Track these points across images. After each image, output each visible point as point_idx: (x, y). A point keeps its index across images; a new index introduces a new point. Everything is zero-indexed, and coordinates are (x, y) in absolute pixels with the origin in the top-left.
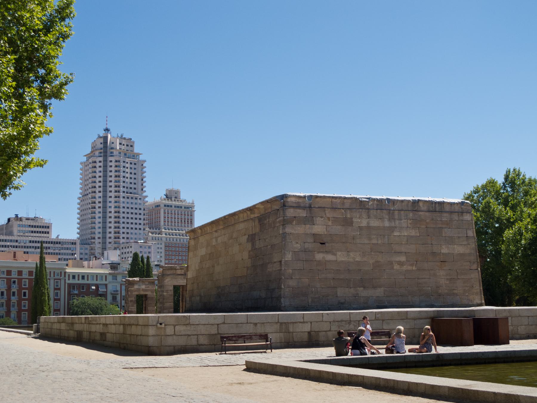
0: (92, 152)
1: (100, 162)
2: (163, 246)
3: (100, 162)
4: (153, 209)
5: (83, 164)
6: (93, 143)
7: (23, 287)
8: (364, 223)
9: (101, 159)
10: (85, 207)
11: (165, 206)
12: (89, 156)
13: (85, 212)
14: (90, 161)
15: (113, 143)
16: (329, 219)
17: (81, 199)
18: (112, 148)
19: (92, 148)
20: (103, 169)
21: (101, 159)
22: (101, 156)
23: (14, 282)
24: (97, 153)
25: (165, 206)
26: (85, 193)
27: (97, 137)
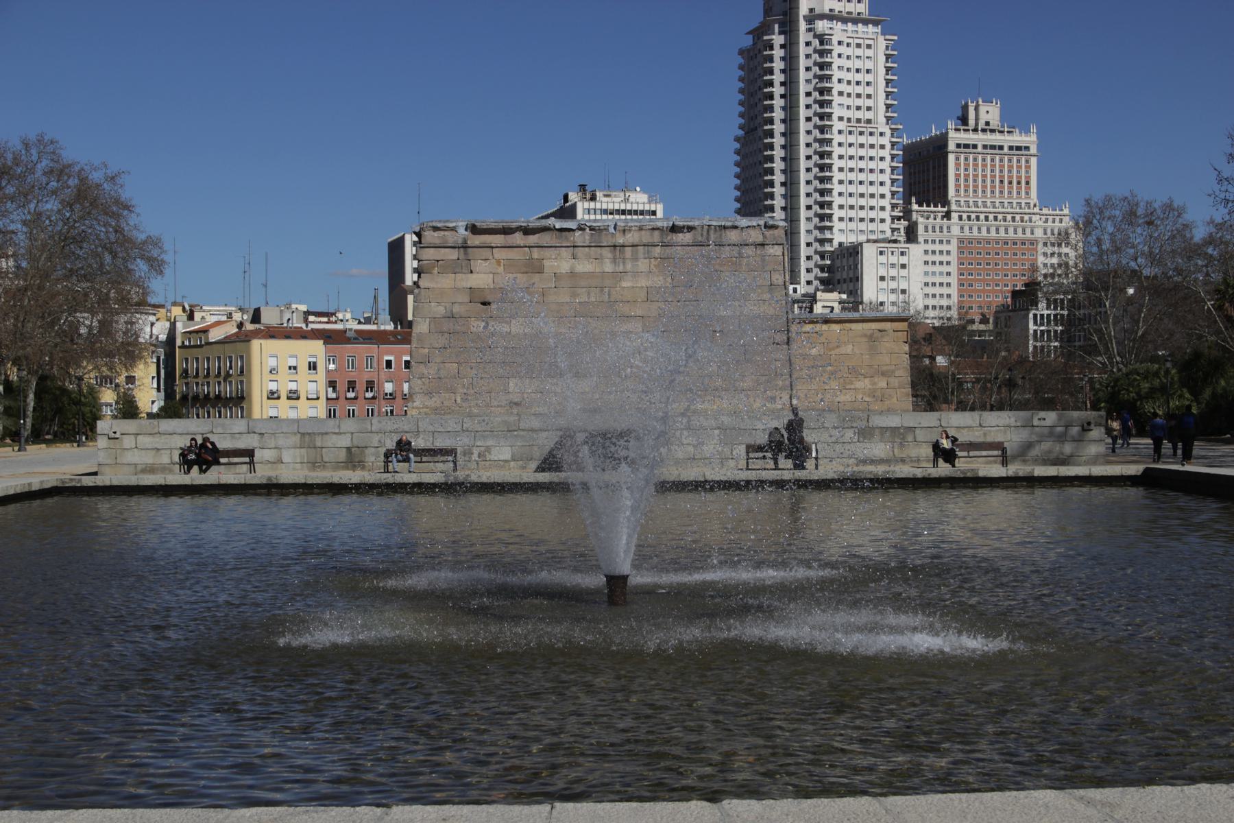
2: (953, 247)
8: (565, 266)
11: (958, 146)
16: (498, 262)
25: (958, 146)
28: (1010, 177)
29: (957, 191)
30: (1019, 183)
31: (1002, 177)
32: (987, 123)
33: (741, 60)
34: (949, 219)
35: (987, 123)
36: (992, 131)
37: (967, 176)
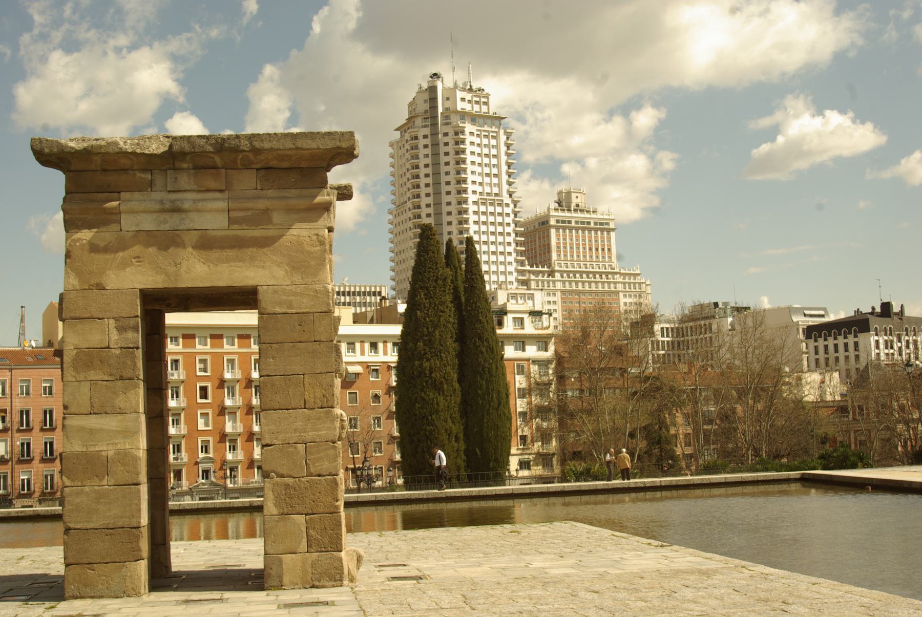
0: (409, 119)
1: (425, 137)
3: (425, 137)
4: (535, 230)
5: (395, 146)
6: (410, 104)
7: (199, 374)
9: (427, 131)
10: (402, 227)
11: (557, 221)
14: (407, 136)
15: (448, 99)
18: (447, 109)
19: (410, 112)
20: (432, 150)
21: (427, 131)
22: (425, 126)
23: (177, 361)
24: (419, 122)
26: (402, 201)
27: (417, 89)
29: (559, 255)
30: (603, 250)
31: (590, 245)
32: (577, 205)
33: (391, 150)
35: (577, 205)
36: (582, 211)
37: (565, 244)
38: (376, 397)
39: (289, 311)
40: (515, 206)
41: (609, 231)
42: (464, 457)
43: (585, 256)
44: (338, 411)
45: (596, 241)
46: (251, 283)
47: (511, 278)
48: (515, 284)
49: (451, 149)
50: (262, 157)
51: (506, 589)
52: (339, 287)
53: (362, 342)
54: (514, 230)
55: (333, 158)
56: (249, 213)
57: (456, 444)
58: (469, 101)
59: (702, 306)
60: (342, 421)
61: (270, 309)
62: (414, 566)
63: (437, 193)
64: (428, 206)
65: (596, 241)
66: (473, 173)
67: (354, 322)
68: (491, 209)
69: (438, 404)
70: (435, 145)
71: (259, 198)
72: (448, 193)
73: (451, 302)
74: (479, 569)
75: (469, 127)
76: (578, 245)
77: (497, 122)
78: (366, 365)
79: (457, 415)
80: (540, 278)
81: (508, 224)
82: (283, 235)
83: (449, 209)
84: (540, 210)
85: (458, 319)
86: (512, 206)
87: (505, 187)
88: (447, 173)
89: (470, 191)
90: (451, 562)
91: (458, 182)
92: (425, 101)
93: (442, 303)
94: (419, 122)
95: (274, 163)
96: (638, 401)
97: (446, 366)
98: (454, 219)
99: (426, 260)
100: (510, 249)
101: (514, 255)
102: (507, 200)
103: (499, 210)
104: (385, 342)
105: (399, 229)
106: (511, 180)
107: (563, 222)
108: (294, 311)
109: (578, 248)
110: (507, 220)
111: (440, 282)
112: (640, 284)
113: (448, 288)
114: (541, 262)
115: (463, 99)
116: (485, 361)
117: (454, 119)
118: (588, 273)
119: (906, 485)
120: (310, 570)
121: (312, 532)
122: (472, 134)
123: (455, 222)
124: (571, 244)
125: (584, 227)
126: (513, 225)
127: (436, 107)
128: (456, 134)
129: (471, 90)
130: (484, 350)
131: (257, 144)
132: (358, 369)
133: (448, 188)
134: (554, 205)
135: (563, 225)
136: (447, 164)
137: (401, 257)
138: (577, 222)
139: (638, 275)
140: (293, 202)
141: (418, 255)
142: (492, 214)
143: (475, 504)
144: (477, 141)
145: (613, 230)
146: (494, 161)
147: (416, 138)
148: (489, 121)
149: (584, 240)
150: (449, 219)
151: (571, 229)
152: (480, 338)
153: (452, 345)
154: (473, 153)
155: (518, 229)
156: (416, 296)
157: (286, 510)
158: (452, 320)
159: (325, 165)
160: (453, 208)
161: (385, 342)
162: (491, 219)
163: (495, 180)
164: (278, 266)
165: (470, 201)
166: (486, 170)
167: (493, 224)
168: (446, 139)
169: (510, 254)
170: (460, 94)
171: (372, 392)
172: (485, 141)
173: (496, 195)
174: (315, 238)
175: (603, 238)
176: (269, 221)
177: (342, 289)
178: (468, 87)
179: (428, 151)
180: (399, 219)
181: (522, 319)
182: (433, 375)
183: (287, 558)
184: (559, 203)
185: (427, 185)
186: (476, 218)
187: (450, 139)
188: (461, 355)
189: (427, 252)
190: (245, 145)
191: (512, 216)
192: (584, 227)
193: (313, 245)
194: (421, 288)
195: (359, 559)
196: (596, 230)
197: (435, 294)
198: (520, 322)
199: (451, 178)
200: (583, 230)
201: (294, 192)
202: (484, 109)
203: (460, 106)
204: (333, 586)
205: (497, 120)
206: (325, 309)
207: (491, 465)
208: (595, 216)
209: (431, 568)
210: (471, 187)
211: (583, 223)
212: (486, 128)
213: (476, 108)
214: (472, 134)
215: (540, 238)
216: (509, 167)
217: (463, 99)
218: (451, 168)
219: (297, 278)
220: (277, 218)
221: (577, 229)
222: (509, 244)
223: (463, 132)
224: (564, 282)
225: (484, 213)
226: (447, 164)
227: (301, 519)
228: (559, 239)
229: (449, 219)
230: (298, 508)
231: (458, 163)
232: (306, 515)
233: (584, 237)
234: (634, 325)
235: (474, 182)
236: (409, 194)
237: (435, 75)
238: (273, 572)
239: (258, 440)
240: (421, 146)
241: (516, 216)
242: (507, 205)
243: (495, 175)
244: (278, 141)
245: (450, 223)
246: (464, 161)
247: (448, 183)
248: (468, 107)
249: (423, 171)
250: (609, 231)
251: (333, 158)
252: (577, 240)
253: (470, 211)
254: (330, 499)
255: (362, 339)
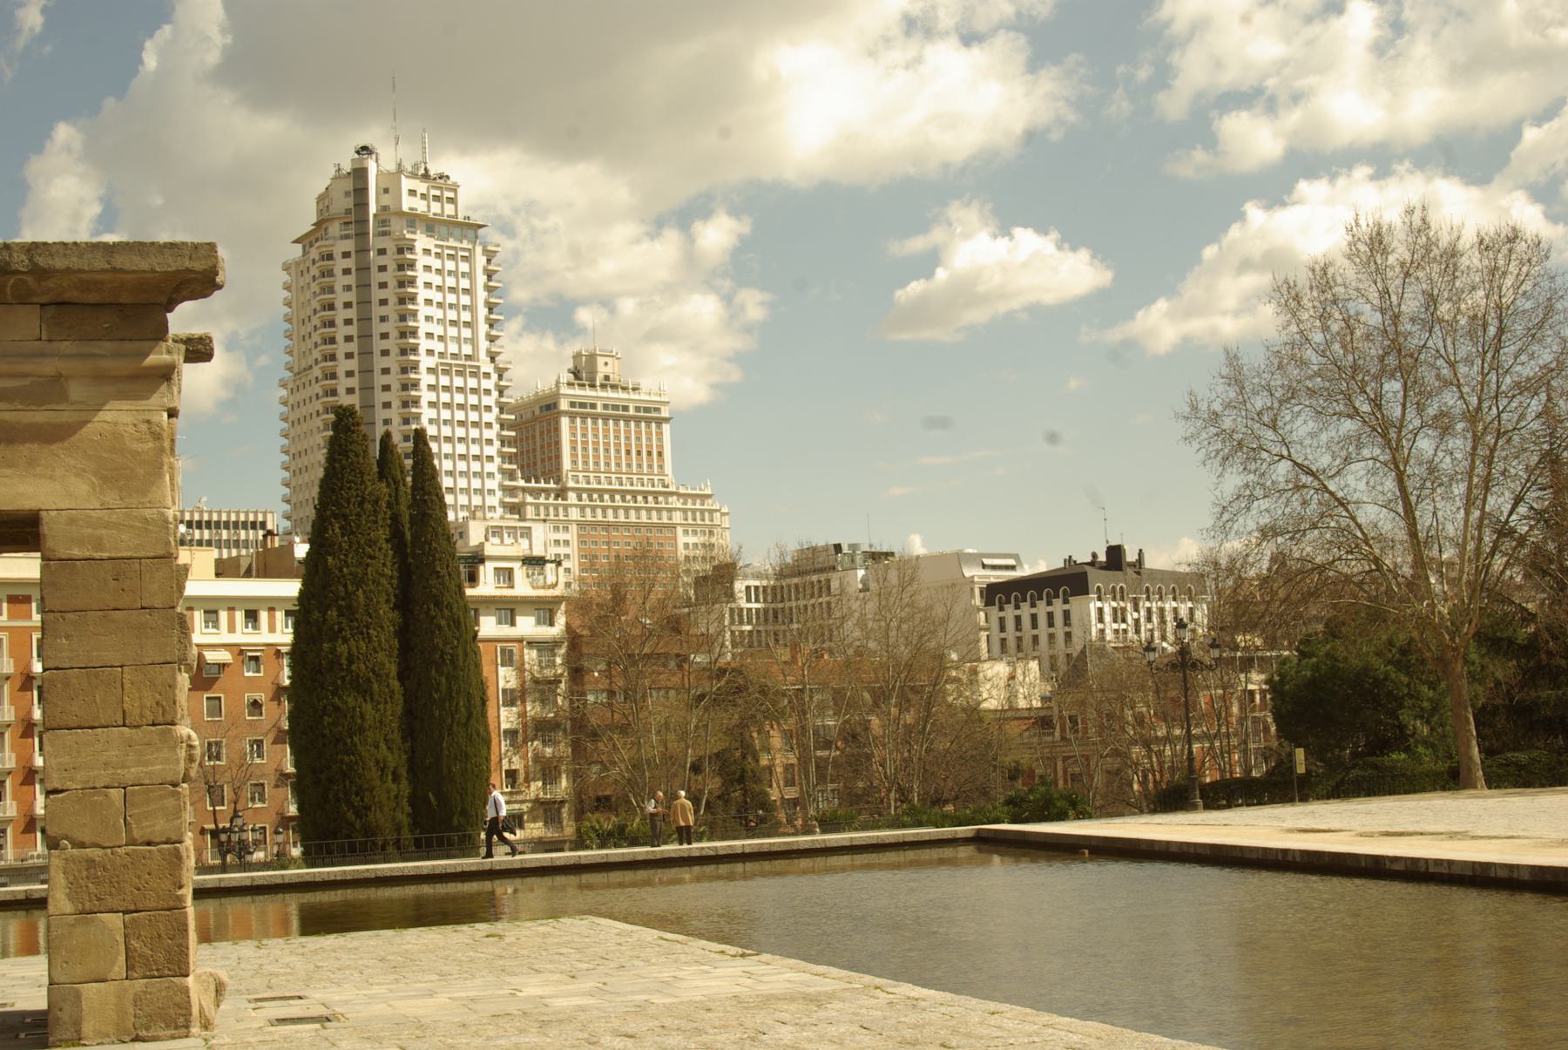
0: (318, 224)
1: (346, 255)
3: (346, 255)
4: (535, 419)
5: (293, 269)
6: (321, 199)
9: (349, 245)
10: (304, 411)
11: (573, 404)
12: (305, 240)
13: (305, 427)
14: (314, 253)
15: (386, 191)
17: (291, 385)
18: (385, 208)
19: (320, 212)
20: (358, 279)
21: (349, 245)
22: (347, 237)
24: (335, 229)
26: (304, 365)
27: (332, 173)
28: (639, 445)
29: (574, 462)
30: (649, 453)
31: (628, 445)
32: (607, 378)
33: (285, 277)
34: (565, 499)
35: (607, 378)
36: (614, 387)
37: (585, 443)
38: (256, 706)
39: (96, 555)
40: (500, 377)
41: (660, 421)
42: (408, 809)
43: (618, 465)
44: (184, 730)
45: (638, 439)
46: (28, 504)
47: (493, 501)
48: (500, 511)
49: (390, 277)
50: (51, 284)
51: (476, 1034)
52: (192, 513)
53: (231, 609)
54: (498, 419)
55: (178, 289)
56: (27, 382)
57: (394, 787)
58: (424, 196)
59: (814, 550)
60: (191, 747)
61: (63, 552)
62: (318, 999)
63: (366, 353)
64: (350, 374)
65: (638, 439)
66: (428, 319)
67: (218, 575)
68: (458, 381)
69: (362, 717)
70: (363, 269)
71: (43, 355)
72: (385, 353)
73: (387, 541)
74: (430, 1001)
75: (422, 241)
76: (607, 444)
77: (471, 233)
78: (239, 650)
79: (397, 736)
80: (542, 500)
81: (488, 409)
82: (87, 422)
83: (385, 380)
84: (544, 385)
85: (400, 570)
86: (495, 376)
87: (484, 345)
88: (383, 319)
89: (422, 350)
90: (382, 990)
91: (403, 335)
92: (347, 194)
93: (372, 543)
94: (335, 229)
95: (72, 295)
96: (706, 709)
97: (377, 648)
98: (394, 397)
99: (343, 468)
100: (490, 451)
101: (498, 460)
102: (486, 366)
103: (472, 383)
104: (271, 610)
105: (298, 414)
106: (494, 333)
107: (583, 405)
108: (105, 555)
109: (607, 450)
110: (486, 401)
111: (368, 506)
112: (711, 512)
113: (380, 516)
114: (543, 474)
115: (412, 192)
116: (445, 644)
117: (396, 226)
118: (623, 493)
119: (1144, 847)
120: (131, 1010)
121: (135, 943)
122: (427, 252)
123: (396, 404)
124: (596, 443)
125: (617, 414)
126: (496, 410)
127: (366, 205)
128: (400, 251)
129: (426, 176)
130: (443, 623)
131: (41, 261)
132: (224, 656)
133: (385, 344)
134: (567, 377)
135: (583, 410)
136: (384, 302)
137: (301, 463)
138: (605, 407)
139: (709, 496)
140: (107, 364)
141: (331, 459)
142: (460, 390)
143: (427, 889)
144: (437, 264)
145: (667, 420)
146: (465, 300)
147: (330, 257)
148: (457, 231)
149: (617, 437)
150: (386, 397)
151: (595, 418)
152: (437, 604)
153: (387, 614)
154: (428, 285)
155: (504, 416)
156: (326, 530)
157: (88, 906)
158: (388, 572)
159: (163, 300)
160: (393, 379)
161: (271, 610)
162: (459, 398)
163: (466, 333)
164: (77, 475)
165: (423, 368)
166: (452, 315)
167: (461, 407)
168: (382, 261)
169: (490, 458)
170: (407, 184)
171: (248, 696)
172: (450, 265)
173: (468, 357)
174: (144, 427)
175: (649, 434)
176: (63, 397)
177: (197, 517)
178: (422, 171)
179: (351, 280)
180: (299, 397)
181: (510, 571)
182: (354, 667)
183: (90, 990)
184: (576, 373)
185: (348, 339)
186: (432, 396)
187: (389, 260)
188: (403, 633)
189: (345, 453)
190: (20, 261)
191: (495, 394)
192: (617, 414)
193: (140, 440)
194: (335, 516)
195: (220, 989)
196: (638, 420)
197: (358, 526)
198: (507, 576)
199: (391, 327)
200: (617, 419)
201: (108, 346)
202: (449, 209)
203: (407, 203)
204: (173, 1038)
205: (470, 229)
206: (161, 552)
207: (455, 821)
208: (636, 397)
209: (346, 1002)
210: (424, 344)
211: (615, 407)
212: (452, 243)
213: (436, 207)
214: (427, 252)
215: (542, 433)
216: (491, 310)
217: (412, 192)
218: (391, 310)
219: (112, 498)
220: (76, 391)
221: (606, 418)
222: (489, 442)
223: (411, 249)
224: (583, 508)
225: (446, 389)
226: (384, 302)
227: (115, 921)
228: (574, 435)
229: (386, 397)
230: (111, 902)
231: (402, 301)
232: (124, 913)
233: (617, 432)
234: (700, 581)
235: (430, 335)
236: (316, 354)
237: (364, 148)
238: (65, 1016)
239: (42, 781)
240: (338, 271)
241: (501, 393)
242: (487, 375)
243: (467, 324)
244: (81, 256)
245: (387, 405)
246: (413, 299)
247: (385, 336)
248: (420, 206)
249: (341, 314)
250: (660, 421)
251: (178, 289)
252: (606, 436)
253: (423, 385)
254: (167, 884)
255: (231, 604)
